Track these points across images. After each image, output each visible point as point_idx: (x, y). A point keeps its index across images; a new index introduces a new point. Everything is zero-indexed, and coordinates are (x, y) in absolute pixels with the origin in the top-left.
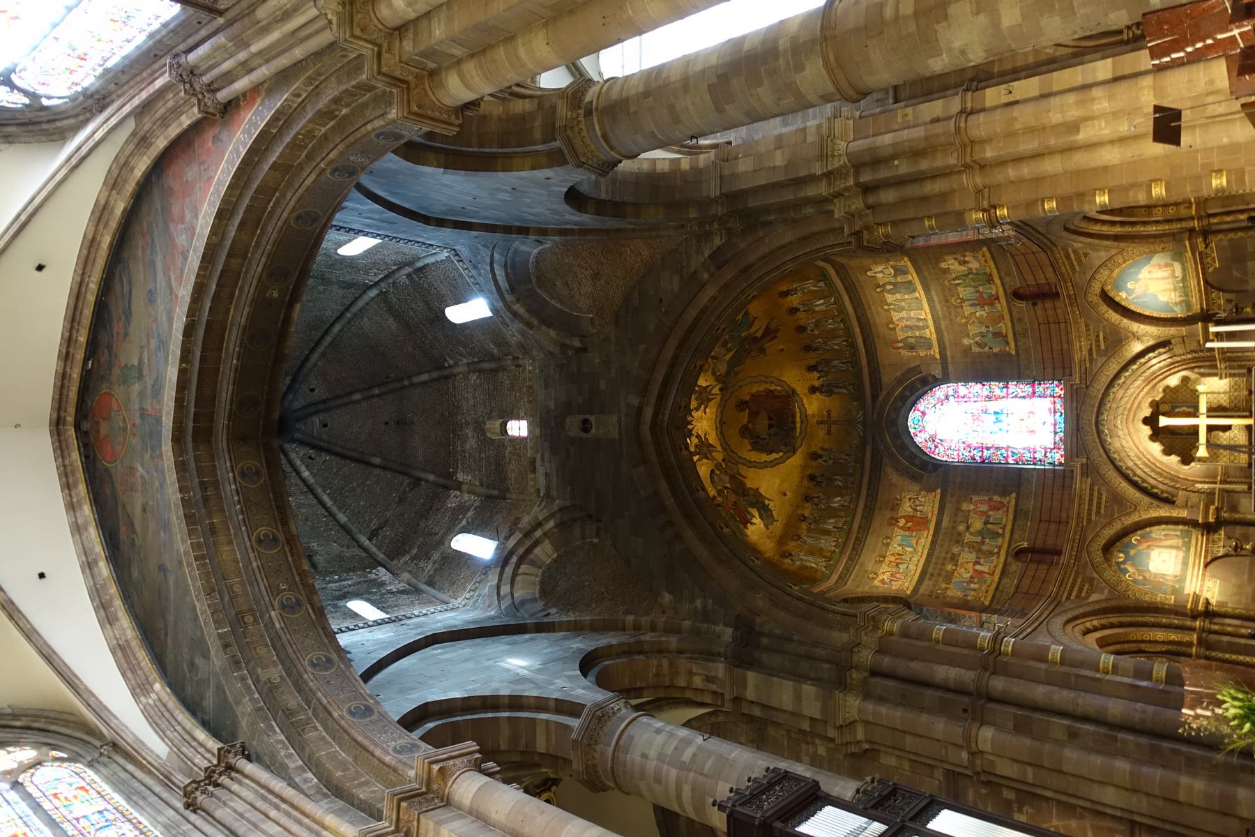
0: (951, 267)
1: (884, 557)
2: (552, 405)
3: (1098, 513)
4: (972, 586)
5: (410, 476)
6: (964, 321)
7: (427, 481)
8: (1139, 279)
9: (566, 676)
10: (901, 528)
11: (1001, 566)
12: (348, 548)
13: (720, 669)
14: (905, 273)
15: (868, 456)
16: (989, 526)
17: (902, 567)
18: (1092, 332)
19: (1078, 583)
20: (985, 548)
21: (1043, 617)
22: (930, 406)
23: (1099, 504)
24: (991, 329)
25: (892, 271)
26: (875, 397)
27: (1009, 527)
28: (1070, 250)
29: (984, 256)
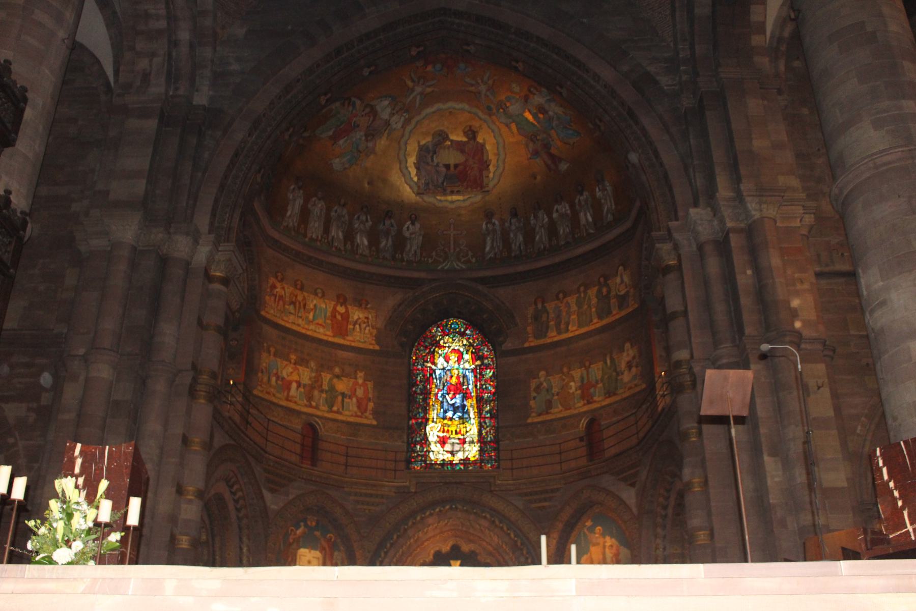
0: (625, 354)
1: (302, 289)
4: (274, 379)
8: (604, 537)
10: (335, 309)
13: (158, 88)
14: (620, 307)
16: (340, 398)
17: (291, 308)
20: (316, 393)
22: (471, 341)
24: (556, 397)
25: (622, 293)
26: (483, 281)
27: (340, 417)
29: (636, 385)
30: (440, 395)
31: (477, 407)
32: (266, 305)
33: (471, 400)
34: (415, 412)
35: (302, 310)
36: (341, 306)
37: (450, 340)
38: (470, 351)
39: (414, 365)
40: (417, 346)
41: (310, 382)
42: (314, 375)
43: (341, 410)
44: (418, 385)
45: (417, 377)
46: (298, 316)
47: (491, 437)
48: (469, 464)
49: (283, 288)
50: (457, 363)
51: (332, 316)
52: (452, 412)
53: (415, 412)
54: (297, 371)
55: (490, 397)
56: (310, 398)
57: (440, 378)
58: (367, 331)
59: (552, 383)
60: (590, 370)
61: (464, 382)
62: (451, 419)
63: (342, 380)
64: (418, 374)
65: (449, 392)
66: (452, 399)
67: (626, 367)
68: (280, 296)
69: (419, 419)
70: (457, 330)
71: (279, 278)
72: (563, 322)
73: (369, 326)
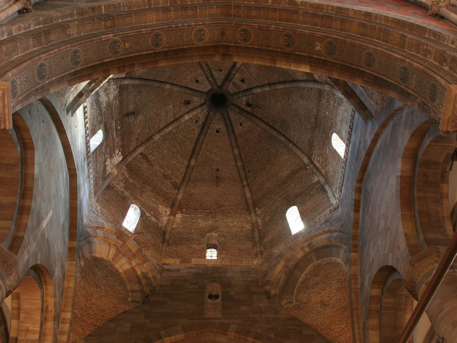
2: (229, 274)
5: (181, 183)
7: (177, 194)
9: (37, 253)
12: (137, 139)
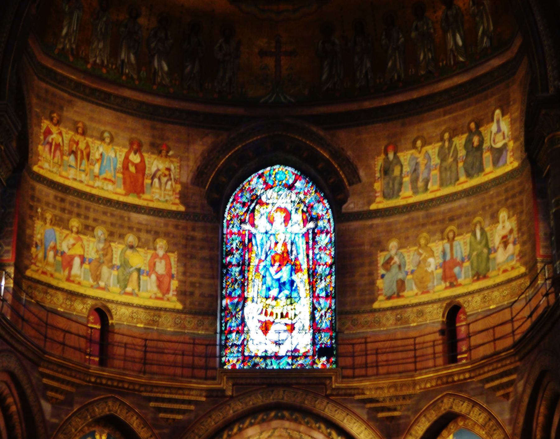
0: (500, 226)
1: (84, 134)
3: (160, 410)
4: (51, 254)
6: (423, 242)
10: (127, 158)
11: (81, 290)
14: (496, 163)
15: (230, 111)
16: (135, 275)
17: (71, 159)
18: (401, 402)
19: (64, 387)
20: (105, 270)
21: (17, 345)
22: (302, 196)
23: (172, 411)
24: (410, 277)
25: (499, 145)
28: (514, 377)
29: (513, 268)
30: (261, 267)
31: (310, 283)
32: (40, 158)
33: (301, 274)
34: (229, 290)
35: (85, 161)
36: (135, 153)
37: (275, 195)
38: (300, 210)
39: (228, 227)
40: (232, 202)
41: (97, 257)
42: (101, 246)
43: (136, 291)
44: (232, 254)
45: (232, 244)
46: (80, 170)
47: (326, 322)
48: (298, 356)
49: (60, 133)
50: (283, 224)
51: (123, 168)
52: (277, 290)
53: (229, 290)
54: (79, 243)
55: (325, 270)
56: (97, 277)
57: (262, 244)
58: (168, 187)
59: (406, 258)
60: (455, 243)
61: (292, 251)
62: (275, 298)
63: (138, 251)
64: (233, 240)
65: (273, 263)
66: (277, 272)
67: (500, 243)
68: (56, 144)
69: (235, 298)
70: (284, 182)
71: (55, 121)
72: (421, 179)
73: (171, 179)
